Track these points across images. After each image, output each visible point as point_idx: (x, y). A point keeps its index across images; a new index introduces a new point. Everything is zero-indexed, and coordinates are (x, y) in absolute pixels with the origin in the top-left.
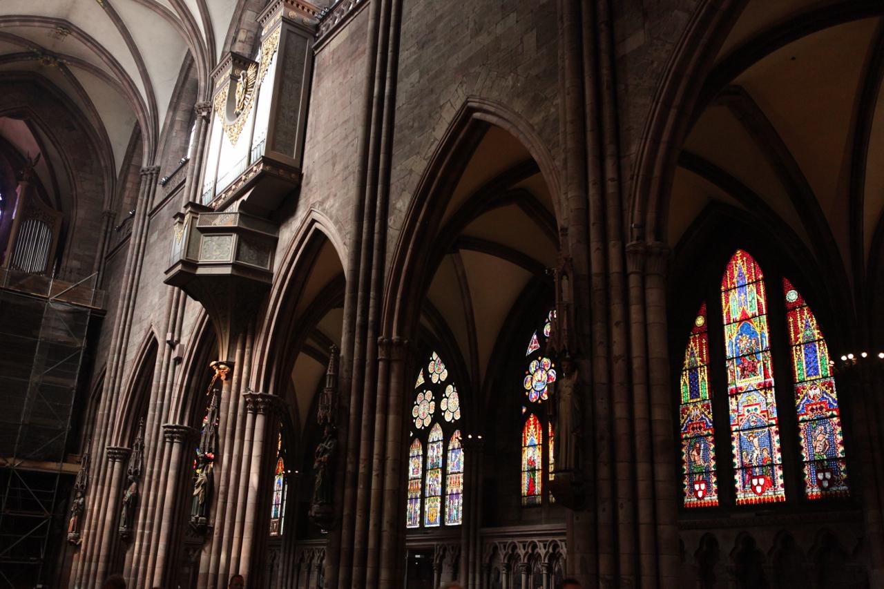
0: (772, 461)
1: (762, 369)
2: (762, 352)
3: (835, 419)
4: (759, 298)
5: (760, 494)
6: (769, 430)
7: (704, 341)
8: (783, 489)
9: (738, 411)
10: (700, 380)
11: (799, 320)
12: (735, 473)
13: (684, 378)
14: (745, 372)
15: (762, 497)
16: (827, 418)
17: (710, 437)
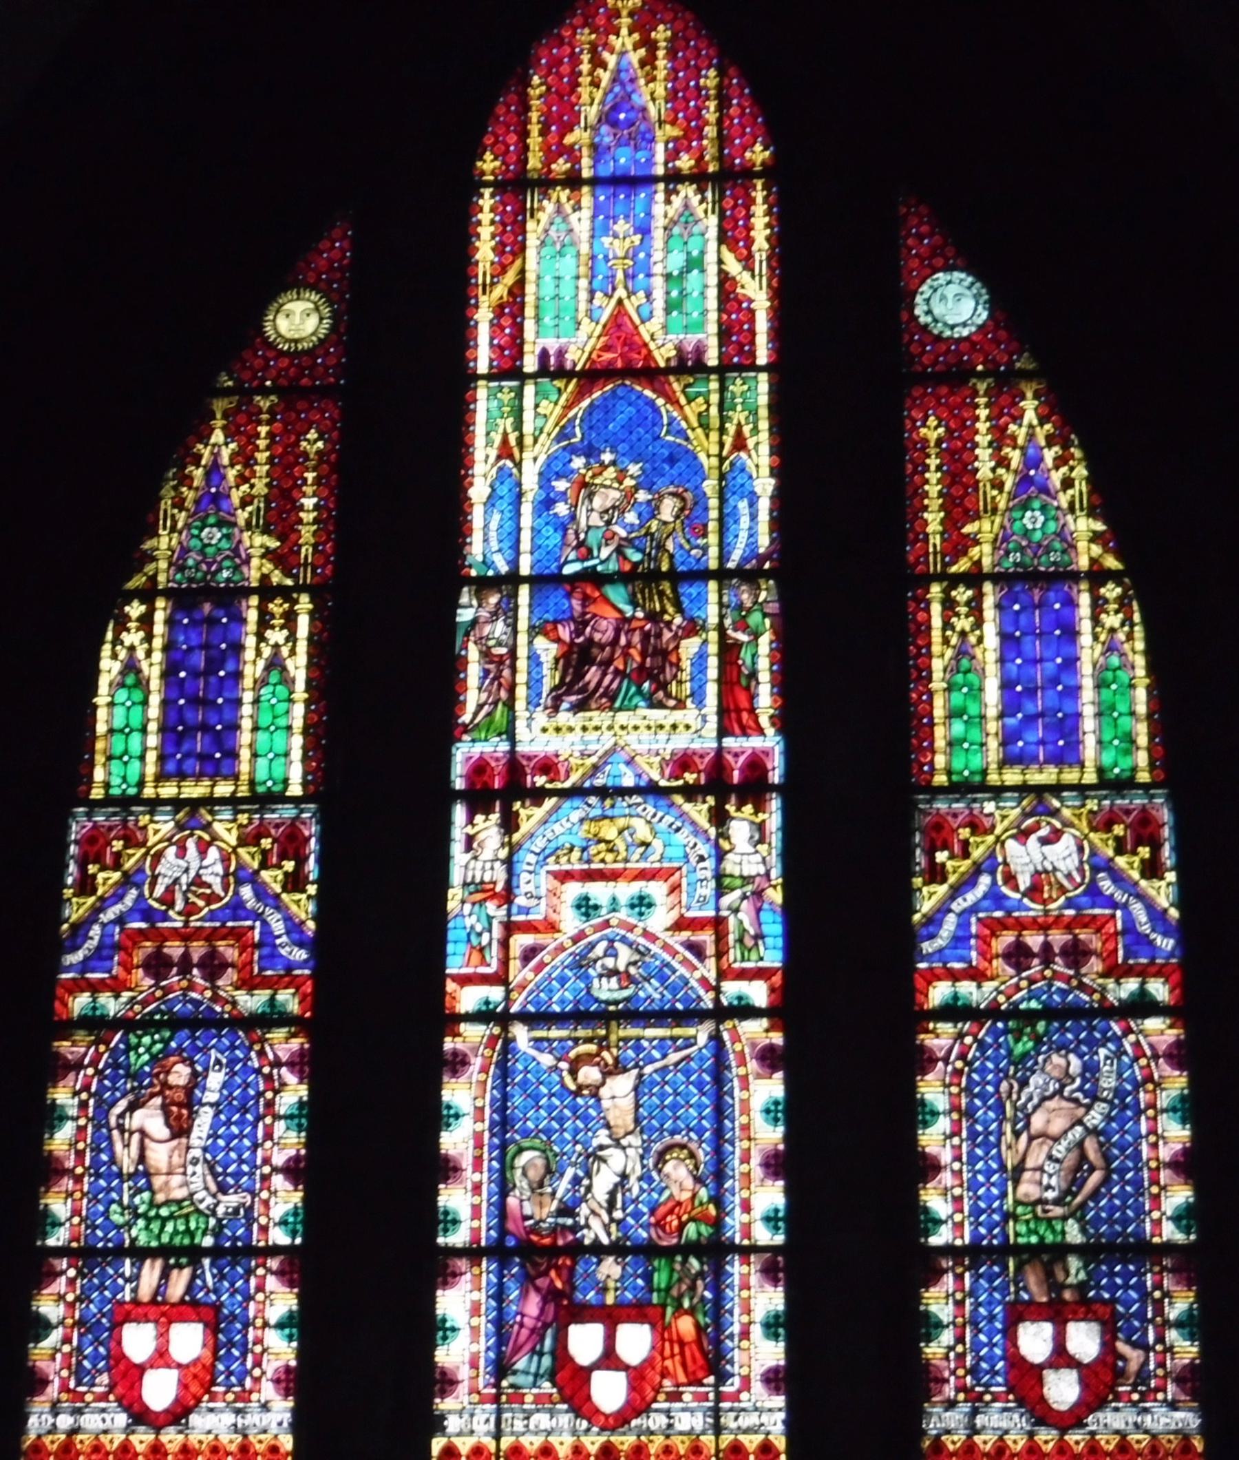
0: (718, 1224)
1: (713, 672)
2: (722, 575)
3: (1153, 1024)
4: (733, 266)
5: (621, 1420)
6: (716, 1038)
7: (313, 443)
8: (779, 1401)
9: (507, 896)
10: (252, 670)
11: (983, 439)
12: (448, 1277)
13: (133, 637)
14: (592, 675)
15: (625, 1441)
16: (1108, 1011)
17: (278, 1034)
